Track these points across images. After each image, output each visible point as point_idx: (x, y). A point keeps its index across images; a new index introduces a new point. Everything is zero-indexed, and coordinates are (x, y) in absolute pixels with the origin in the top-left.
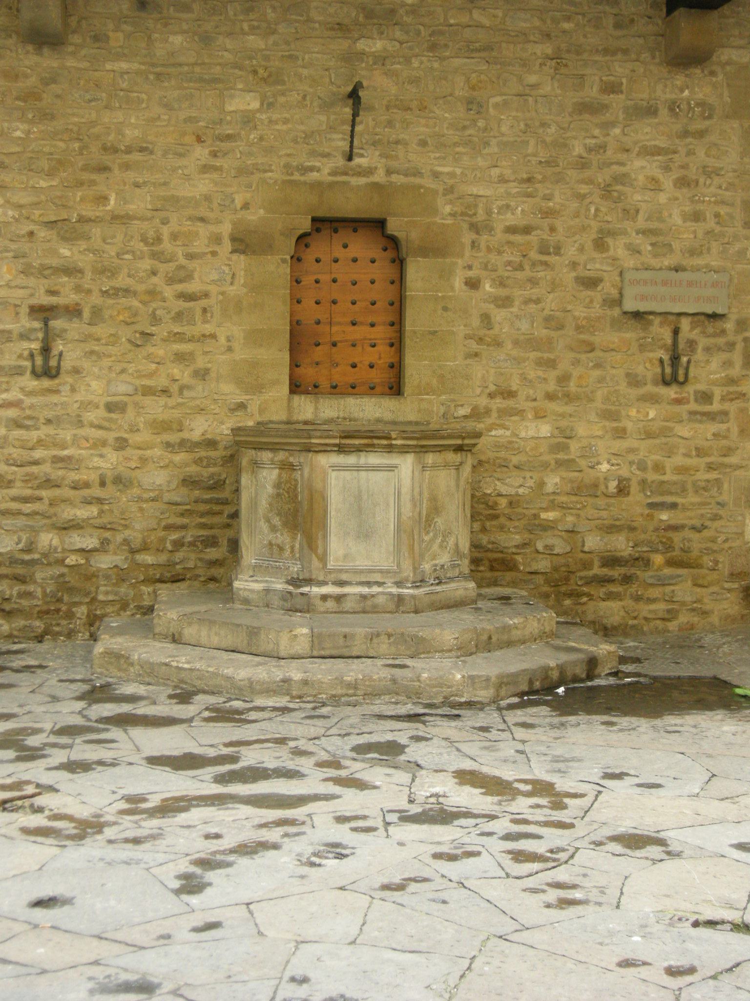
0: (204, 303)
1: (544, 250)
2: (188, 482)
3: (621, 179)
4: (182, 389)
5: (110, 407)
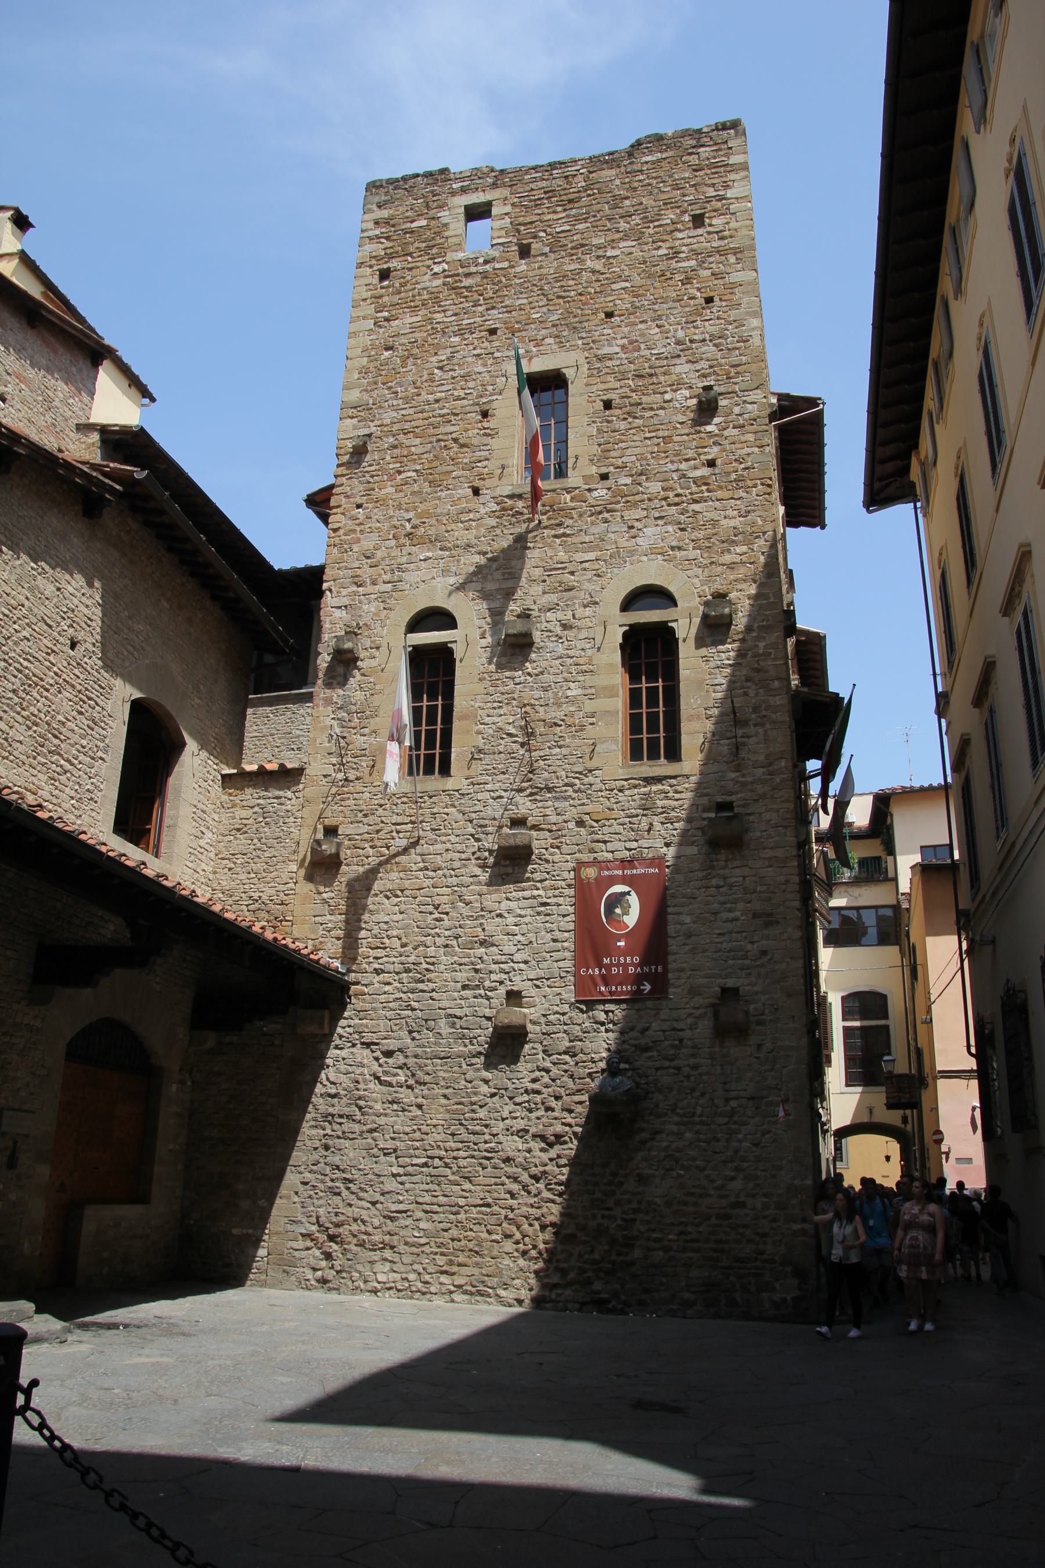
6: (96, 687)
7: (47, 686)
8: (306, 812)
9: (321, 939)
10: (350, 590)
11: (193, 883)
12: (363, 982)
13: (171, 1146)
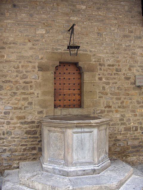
0: (31, 84)
1: (117, 70)
2: (28, 133)
3: (134, 54)
4: (25, 107)
5: (5, 113)
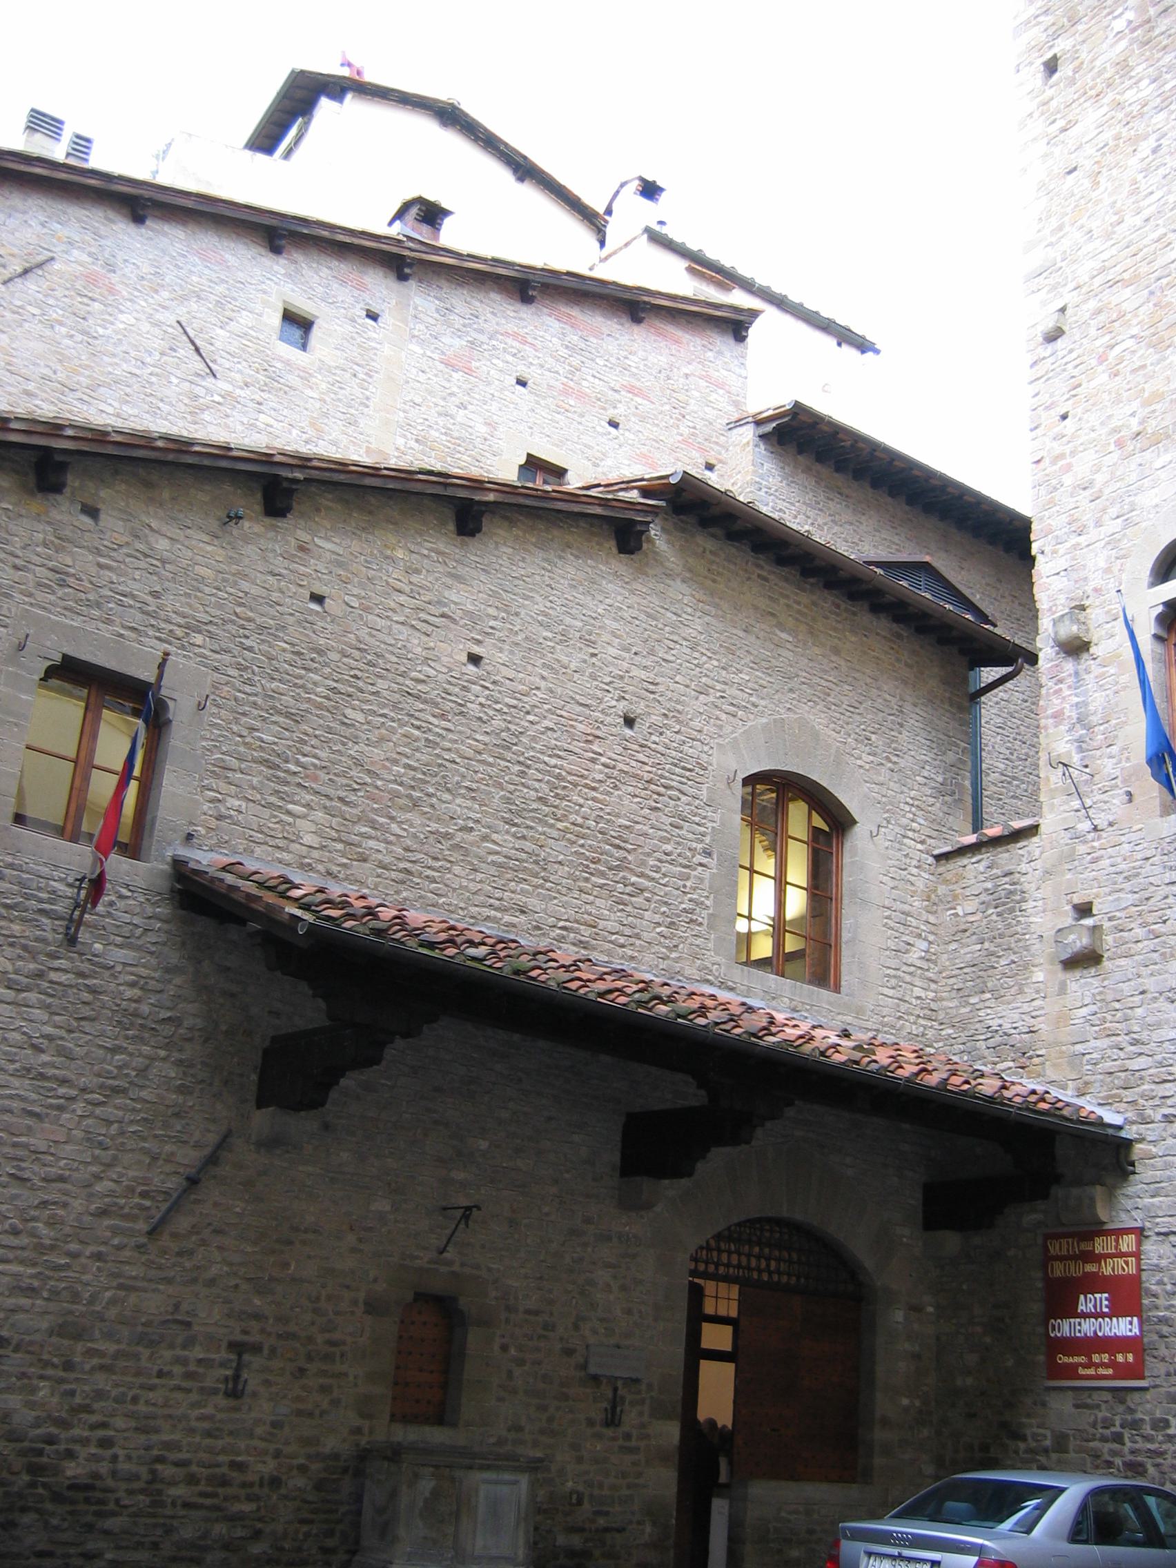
4: (322, 1413)
5: (274, 1425)
6: (677, 770)
7: (593, 785)
8: (1047, 890)
9: (1086, 1078)
10: (1068, 545)
11: (900, 1018)
12: (1149, 1138)
13: (905, 1401)
